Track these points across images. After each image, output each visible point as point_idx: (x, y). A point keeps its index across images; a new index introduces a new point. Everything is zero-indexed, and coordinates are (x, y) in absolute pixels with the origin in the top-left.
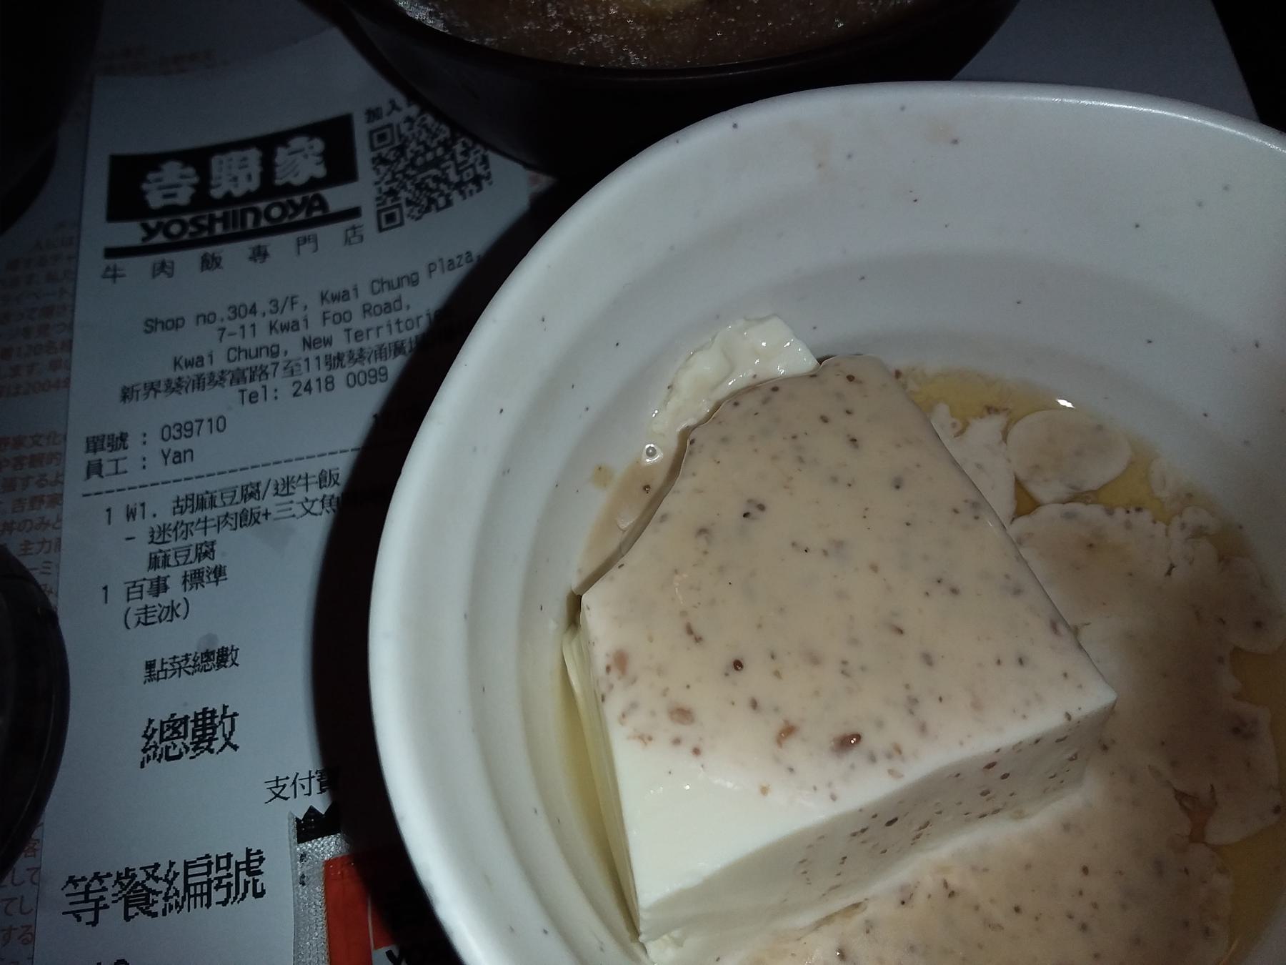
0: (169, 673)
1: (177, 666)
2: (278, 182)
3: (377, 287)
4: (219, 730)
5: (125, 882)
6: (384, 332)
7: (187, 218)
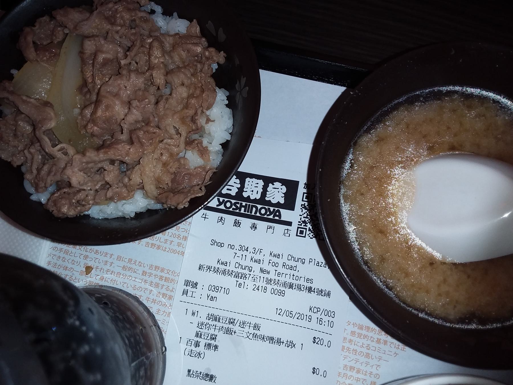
0: (195, 376)
1: (197, 375)
2: (267, 199)
3: (290, 258)
6: (288, 276)
7: (233, 201)
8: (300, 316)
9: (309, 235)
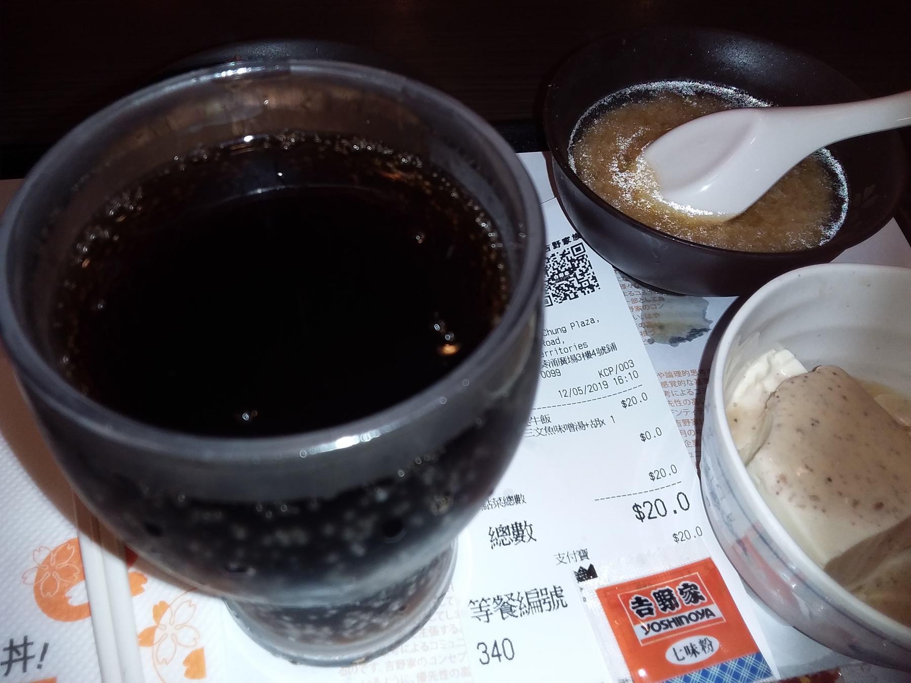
4: (525, 532)
5: (498, 602)
6: (554, 353)
8: (592, 388)
9: (556, 301)
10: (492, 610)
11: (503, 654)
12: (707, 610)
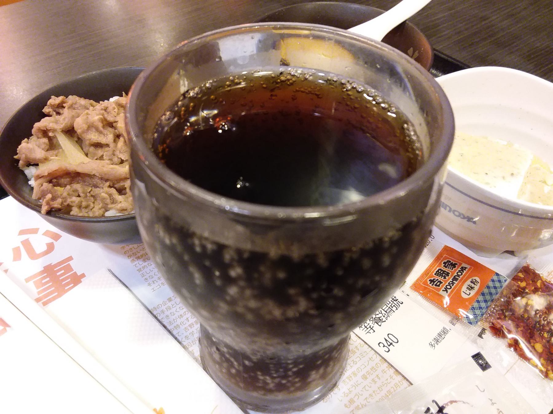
5: (372, 319)
10: (372, 325)
11: (393, 342)
12: (462, 267)
